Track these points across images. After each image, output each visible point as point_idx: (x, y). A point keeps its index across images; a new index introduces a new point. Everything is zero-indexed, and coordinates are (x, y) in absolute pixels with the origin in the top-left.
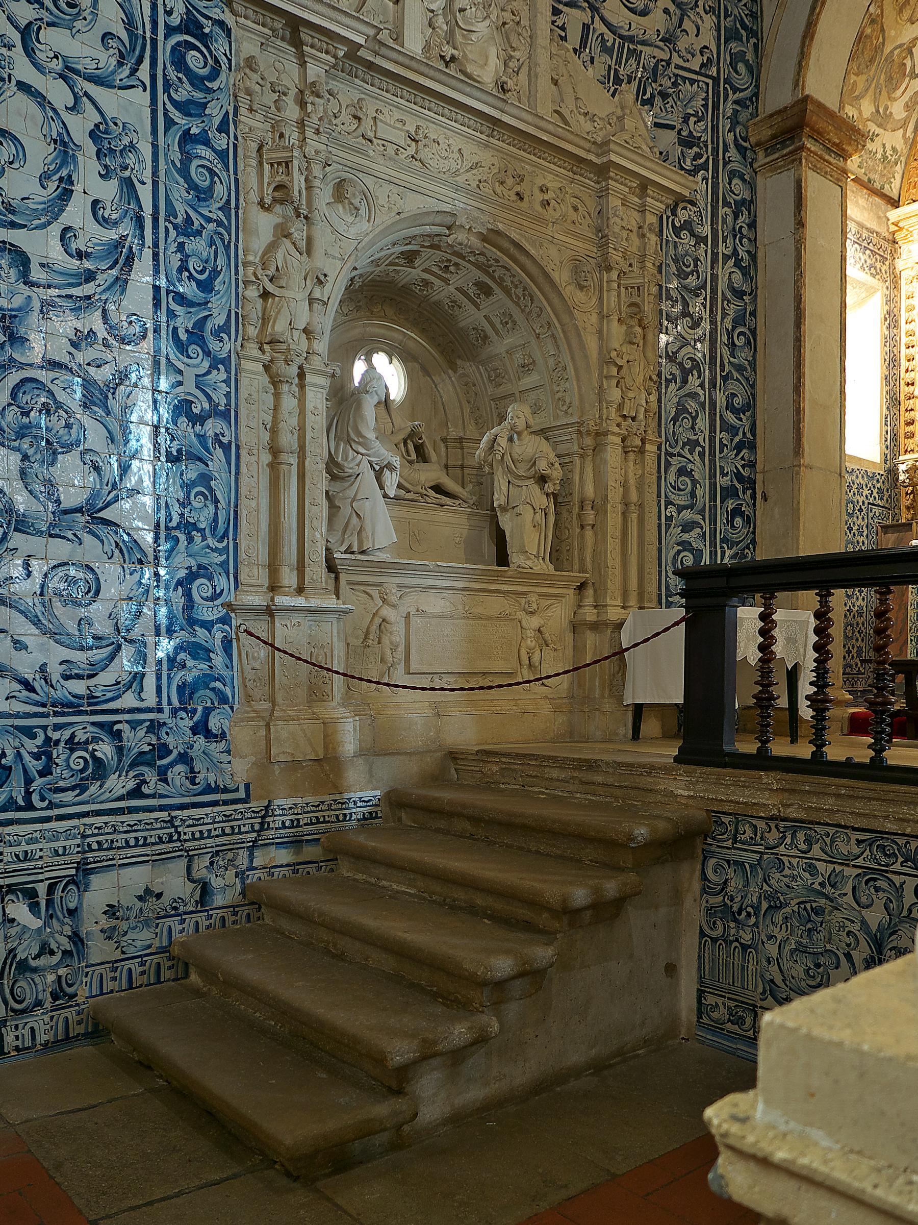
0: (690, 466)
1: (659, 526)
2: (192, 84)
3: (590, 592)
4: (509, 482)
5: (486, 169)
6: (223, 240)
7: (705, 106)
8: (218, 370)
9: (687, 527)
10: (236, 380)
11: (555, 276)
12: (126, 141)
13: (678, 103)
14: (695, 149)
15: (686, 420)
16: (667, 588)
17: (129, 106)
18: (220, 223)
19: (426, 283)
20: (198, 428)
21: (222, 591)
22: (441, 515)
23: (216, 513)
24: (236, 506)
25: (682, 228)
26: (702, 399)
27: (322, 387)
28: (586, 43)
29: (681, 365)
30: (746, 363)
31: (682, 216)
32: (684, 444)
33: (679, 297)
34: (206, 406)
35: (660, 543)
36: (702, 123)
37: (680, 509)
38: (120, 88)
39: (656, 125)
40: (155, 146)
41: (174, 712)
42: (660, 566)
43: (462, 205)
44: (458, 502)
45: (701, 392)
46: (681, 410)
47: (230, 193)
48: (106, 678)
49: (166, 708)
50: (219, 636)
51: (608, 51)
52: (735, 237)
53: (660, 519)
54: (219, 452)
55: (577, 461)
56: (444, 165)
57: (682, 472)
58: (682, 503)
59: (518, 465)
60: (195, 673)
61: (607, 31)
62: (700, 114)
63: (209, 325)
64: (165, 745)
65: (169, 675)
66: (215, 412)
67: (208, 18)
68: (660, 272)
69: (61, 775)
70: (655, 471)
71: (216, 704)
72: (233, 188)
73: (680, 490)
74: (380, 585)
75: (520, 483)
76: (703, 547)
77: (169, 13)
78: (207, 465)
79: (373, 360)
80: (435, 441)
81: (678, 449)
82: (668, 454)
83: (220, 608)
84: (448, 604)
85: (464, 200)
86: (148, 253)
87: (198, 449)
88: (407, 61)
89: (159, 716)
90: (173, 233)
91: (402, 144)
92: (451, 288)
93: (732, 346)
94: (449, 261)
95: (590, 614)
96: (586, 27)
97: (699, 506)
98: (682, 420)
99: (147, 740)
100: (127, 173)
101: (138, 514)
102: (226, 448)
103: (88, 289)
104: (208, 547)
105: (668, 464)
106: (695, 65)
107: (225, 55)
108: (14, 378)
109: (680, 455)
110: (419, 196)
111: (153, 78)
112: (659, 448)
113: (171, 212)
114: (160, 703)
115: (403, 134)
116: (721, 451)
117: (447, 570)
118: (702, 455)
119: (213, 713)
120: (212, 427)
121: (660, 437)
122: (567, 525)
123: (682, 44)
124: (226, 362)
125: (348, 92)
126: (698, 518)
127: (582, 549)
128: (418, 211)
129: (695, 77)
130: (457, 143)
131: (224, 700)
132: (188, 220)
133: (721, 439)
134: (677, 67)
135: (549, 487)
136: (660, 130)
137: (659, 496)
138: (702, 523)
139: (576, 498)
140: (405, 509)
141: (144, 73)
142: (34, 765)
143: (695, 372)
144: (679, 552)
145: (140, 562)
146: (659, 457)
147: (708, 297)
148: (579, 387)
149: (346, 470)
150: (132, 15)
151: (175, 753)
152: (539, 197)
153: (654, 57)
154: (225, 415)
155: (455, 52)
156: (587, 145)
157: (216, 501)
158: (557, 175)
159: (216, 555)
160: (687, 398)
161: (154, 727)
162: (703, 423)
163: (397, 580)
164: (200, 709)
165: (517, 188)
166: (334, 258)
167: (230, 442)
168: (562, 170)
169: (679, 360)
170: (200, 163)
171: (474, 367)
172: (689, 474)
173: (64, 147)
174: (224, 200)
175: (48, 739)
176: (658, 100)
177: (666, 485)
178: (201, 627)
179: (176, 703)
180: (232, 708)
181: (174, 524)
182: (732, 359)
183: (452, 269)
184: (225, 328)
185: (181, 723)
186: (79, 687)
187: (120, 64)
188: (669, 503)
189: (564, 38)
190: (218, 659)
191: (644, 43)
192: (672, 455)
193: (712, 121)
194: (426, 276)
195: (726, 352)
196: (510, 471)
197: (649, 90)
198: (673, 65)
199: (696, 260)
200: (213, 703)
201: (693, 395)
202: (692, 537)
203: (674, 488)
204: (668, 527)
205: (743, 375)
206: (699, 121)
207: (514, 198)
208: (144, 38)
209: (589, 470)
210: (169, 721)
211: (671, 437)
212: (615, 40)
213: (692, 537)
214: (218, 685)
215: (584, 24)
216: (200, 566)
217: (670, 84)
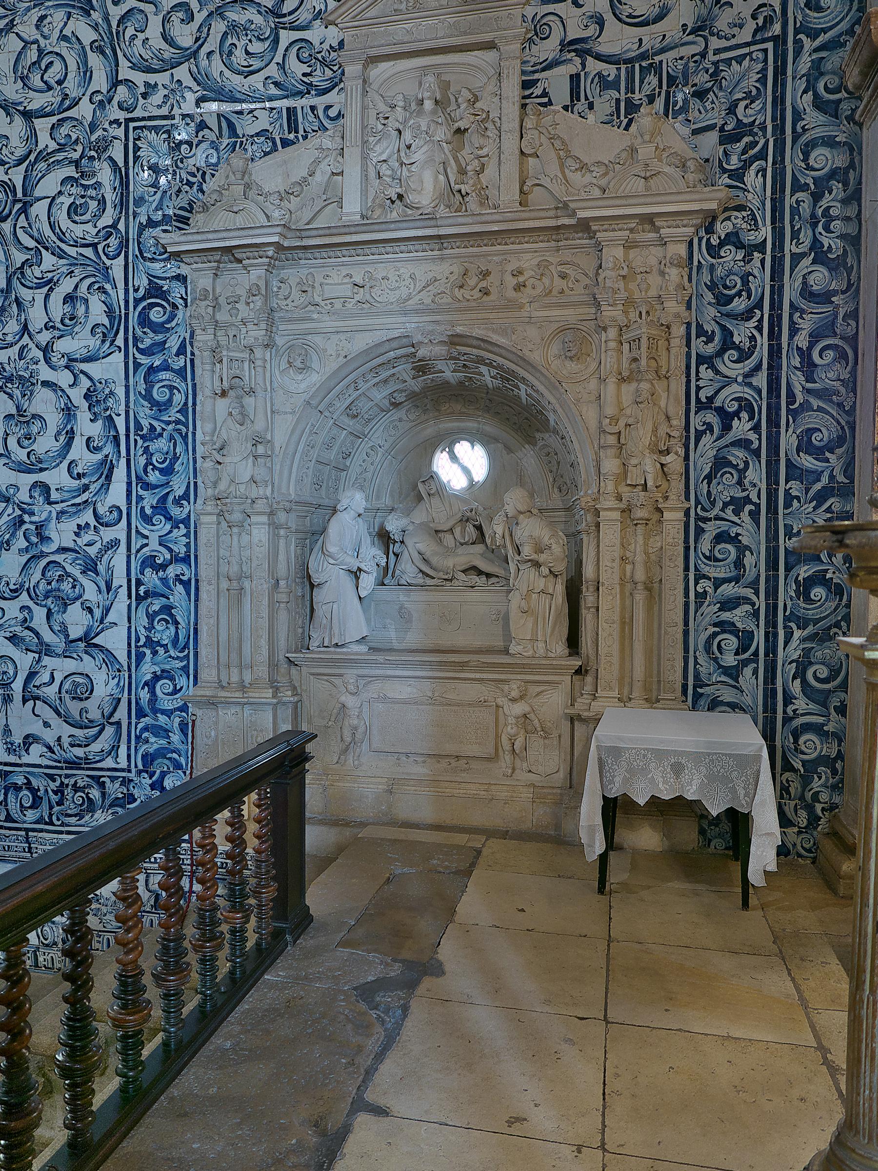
0: (733, 531)
1: (687, 605)
2: (154, 332)
3: (589, 679)
5: (444, 280)
6: (181, 434)
7: (763, 80)
8: (179, 528)
9: (728, 605)
10: (196, 532)
11: (536, 357)
12: (107, 391)
13: (720, 94)
14: (746, 139)
15: (728, 475)
16: (697, 676)
17: (110, 369)
18: (178, 422)
20: (161, 574)
21: (182, 688)
23: (177, 632)
24: (196, 624)
25: (722, 244)
26: (755, 445)
28: (578, 93)
30: (837, 384)
31: (722, 229)
32: (726, 505)
33: (717, 330)
34: (168, 556)
35: (686, 623)
36: (758, 102)
37: (718, 583)
38: (103, 358)
39: (695, 132)
40: (127, 387)
41: (139, 772)
42: (686, 650)
43: (413, 325)
45: (753, 436)
46: (720, 463)
47: (187, 398)
48: (96, 747)
49: (134, 770)
50: (177, 720)
51: (615, 85)
52: (814, 225)
53: (687, 595)
54: (180, 588)
56: (393, 297)
57: (721, 538)
58: (722, 575)
60: (155, 746)
61: (603, 66)
62: (754, 92)
63: (171, 498)
64: (132, 795)
65: (136, 747)
66: (176, 559)
67: (165, 279)
68: (689, 307)
69: (70, 806)
70: (681, 541)
71: (171, 769)
72: (190, 391)
73: (717, 560)
74: (341, 675)
76: (754, 628)
77: (136, 290)
78: (168, 599)
79: (456, 451)
81: (715, 512)
82: (698, 518)
83: (179, 700)
84: (415, 691)
85: (416, 319)
86: (123, 461)
87: (160, 588)
88: (327, 232)
89: (129, 775)
90: (140, 442)
91: (350, 294)
93: (809, 368)
96: (575, 79)
97: (750, 574)
98: (722, 476)
99: (121, 790)
100: (108, 413)
101: (115, 640)
102: (186, 584)
103: (85, 497)
104: (170, 657)
105: (700, 531)
106: (746, 35)
107: (182, 298)
108: (43, 562)
109: (717, 518)
110: (368, 333)
111: (126, 340)
113: (139, 427)
114: (129, 766)
115: (349, 286)
116: (787, 505)
117: (400, 662)
118: (755, 515)
119: (168, 776)
120: (172, 571)
121: (688, 499)
123: (722, 23)
124: (186, 521)
125: (293, 274)
126: (749, 593)
128: (368, 347)
129: (746, 50)
130: (406, 270)
131: (178, 766)
132: (152, 428)
133: (787, 492)
134: (717, 52)
136: (700, 137)
137: (687, 569)
138: (754, 598)
140: (434, 593)
141: (120, 341)
142: (54, 798)
143: (744, 415)
144: (715, 635)
145: (119, 671)
150: (112, 305)
151: (139, 801)
152: (511, 281)
153: (681, 58)
154: (186, 560)
155: (399, 190)
156: (552, 213)
157: (177, 623)
158: (536, 252)
159: (177, 661)
161: (126, 782)
162: (757, 474)
163: (355, 672)
164: (158, 772)
165: (483, 284)
166: (286, 413)
167: (190, 580)
168: (541, 245)
169: (718, 403)
170: (162, 384)
172: (735, 540)
173: (69, 412)
174: (182, 404)
175: (62, 783)
176: (695, 104)
178: (162, 714)
179: (140, 767)
180: (185, 773)
181: (141, 643)
182: (809, 385)
184: (186, 496)
185: (144, 781)
186: (79, 752)
187: (103, 342)
188: (700, 576)
189: (550, 103)
190: (176, 738)
191: (663, 51)
192: (706, 520)
193: (774, 92)
195: (798, 380)
197: (680, 97)
198: (711, 53)
199: (745, 278)
200: (169, 768)
201: (744, 444)
202: (738, 616)
203: (708, 558)
204: (699, 605)
205: (831, 401)
206: (752, 102)
207: (480, 294)
208: (120, 315)
210: (135, 779)
211: (704, 500)
212: (619, 69)
213: (738, 616)
214: (175, 755)
215: (571, 76)
216: (163, 671)
217: (707, 77)
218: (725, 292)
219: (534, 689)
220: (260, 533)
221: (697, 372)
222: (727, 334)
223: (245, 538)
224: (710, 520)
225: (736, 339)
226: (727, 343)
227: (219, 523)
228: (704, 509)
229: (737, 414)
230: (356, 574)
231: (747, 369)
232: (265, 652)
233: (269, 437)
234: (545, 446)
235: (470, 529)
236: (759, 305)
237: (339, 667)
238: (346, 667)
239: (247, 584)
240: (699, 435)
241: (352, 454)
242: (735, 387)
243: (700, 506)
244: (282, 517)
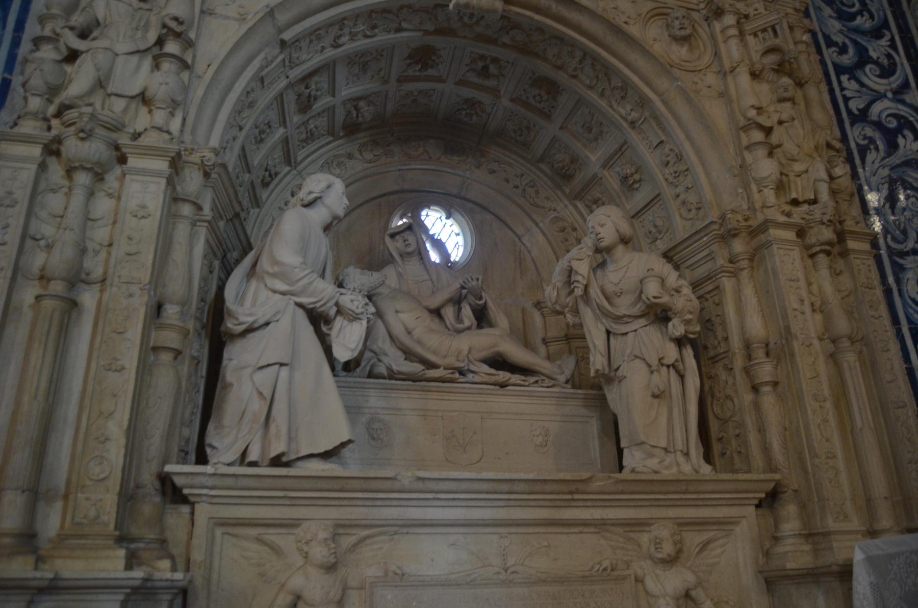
3: (790, 509)
4: (608, 333)
19: (471, 104)
22: (503, 402)
27: (156, 174)
29: (878, 125)
33: (847, 42)
44: (532, 379)
55: (728, 284)
59: (617, 301)
70: (876, 282)
75: (623, 329)
80: (524, 311)
92: (505, 102)
94: (482, 57)
95: (795, 555)
105: (899, 270)
112: (875, 245)
122: (729, 391)
127: (762, 430)
135: (677, 328)
137: (895, 321)
139: (736, 343)
146: (878, 259)
147: (897, 38)
148: (707, 174)
149: (243, 319)
160: (905, 169)
166: (226, 18)
171: (571, 207)
177: (904, 304)
183: (493, 69)
192: (903, 254)
194: (467, 93)
196: (606, 314)
209: (749, 291)
218: (845, 9)
219: (693, 539)
220: (143, 190)
221: (840, 82)
222: (862, 52)
223: (103, 206)
224: (907, 254)
225: (874, 55)
226: (863, 59)
227: (43, 167)
228: (894, 239)
229: (899, 130)
230: (318, 320)
231: (894, 86)
232: (116, 453)
233: (192, 35)
234: (557, 219)
235: (467, 311)
236: (885, 25)
237: (294, 502)
238: (311, 502)
239: (88, 298)
240: (863, 151)
241: (280, 176)
242: (885, 103)
243: (889, 237)
244: (192, 181)
